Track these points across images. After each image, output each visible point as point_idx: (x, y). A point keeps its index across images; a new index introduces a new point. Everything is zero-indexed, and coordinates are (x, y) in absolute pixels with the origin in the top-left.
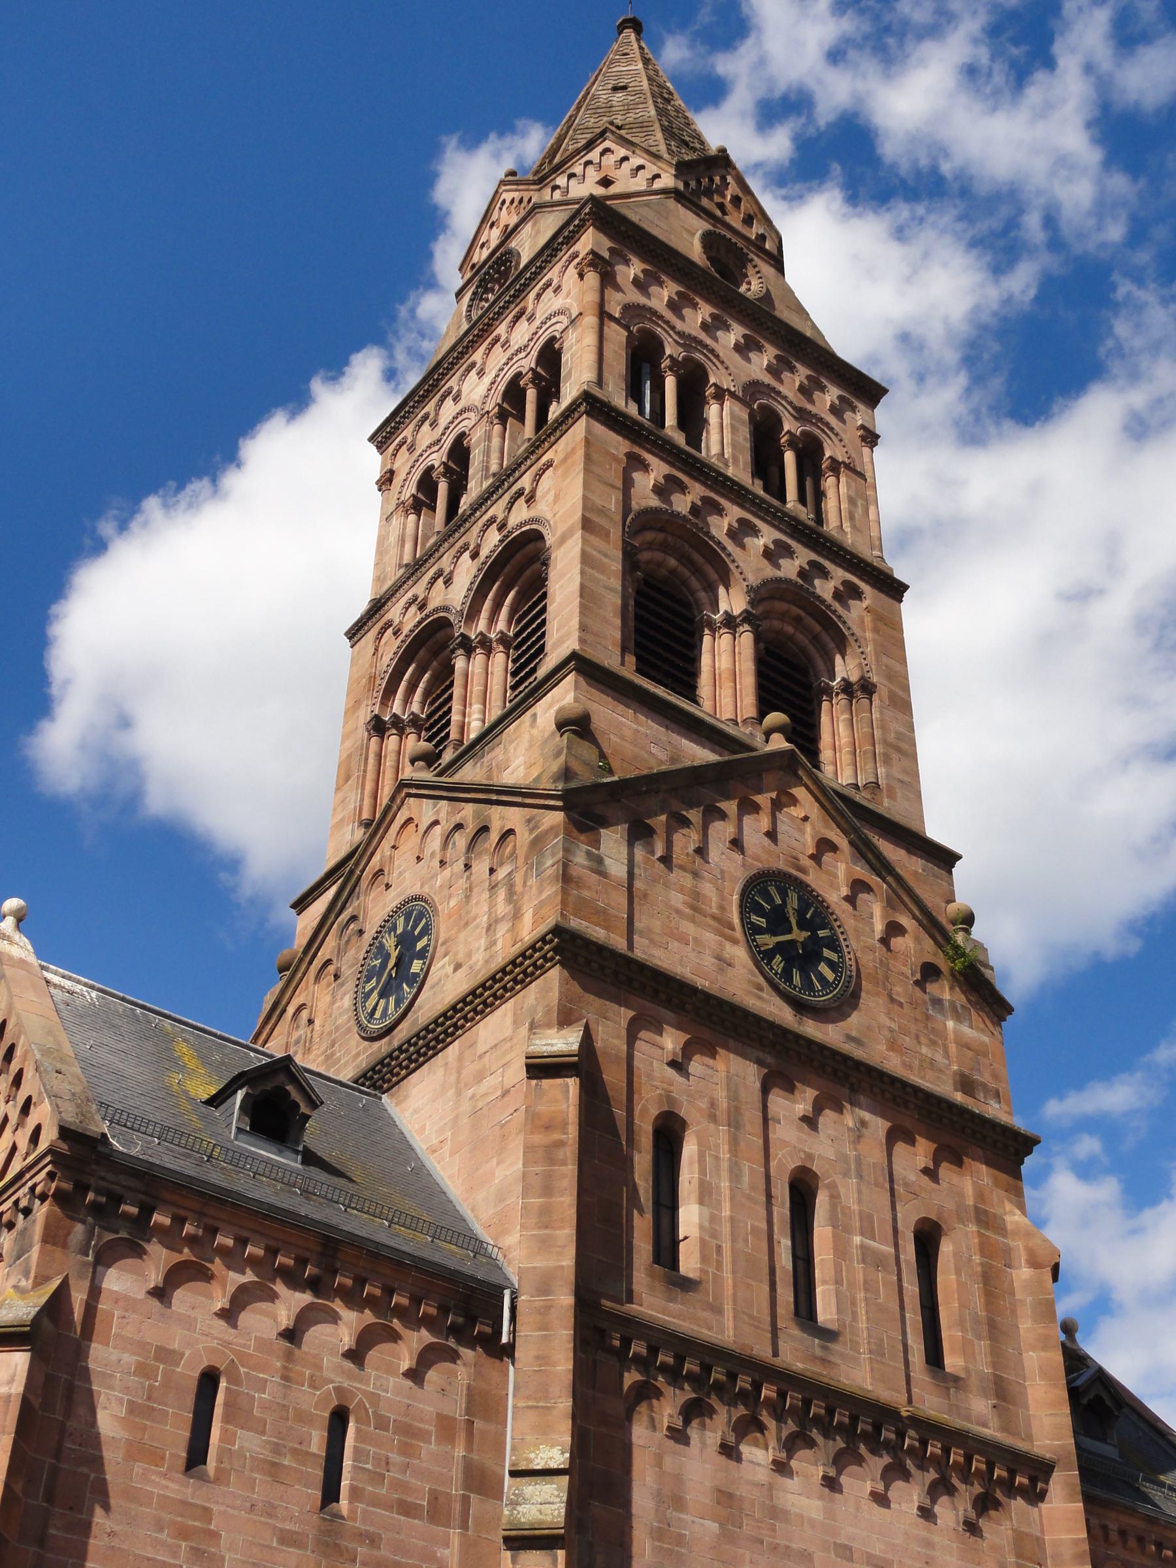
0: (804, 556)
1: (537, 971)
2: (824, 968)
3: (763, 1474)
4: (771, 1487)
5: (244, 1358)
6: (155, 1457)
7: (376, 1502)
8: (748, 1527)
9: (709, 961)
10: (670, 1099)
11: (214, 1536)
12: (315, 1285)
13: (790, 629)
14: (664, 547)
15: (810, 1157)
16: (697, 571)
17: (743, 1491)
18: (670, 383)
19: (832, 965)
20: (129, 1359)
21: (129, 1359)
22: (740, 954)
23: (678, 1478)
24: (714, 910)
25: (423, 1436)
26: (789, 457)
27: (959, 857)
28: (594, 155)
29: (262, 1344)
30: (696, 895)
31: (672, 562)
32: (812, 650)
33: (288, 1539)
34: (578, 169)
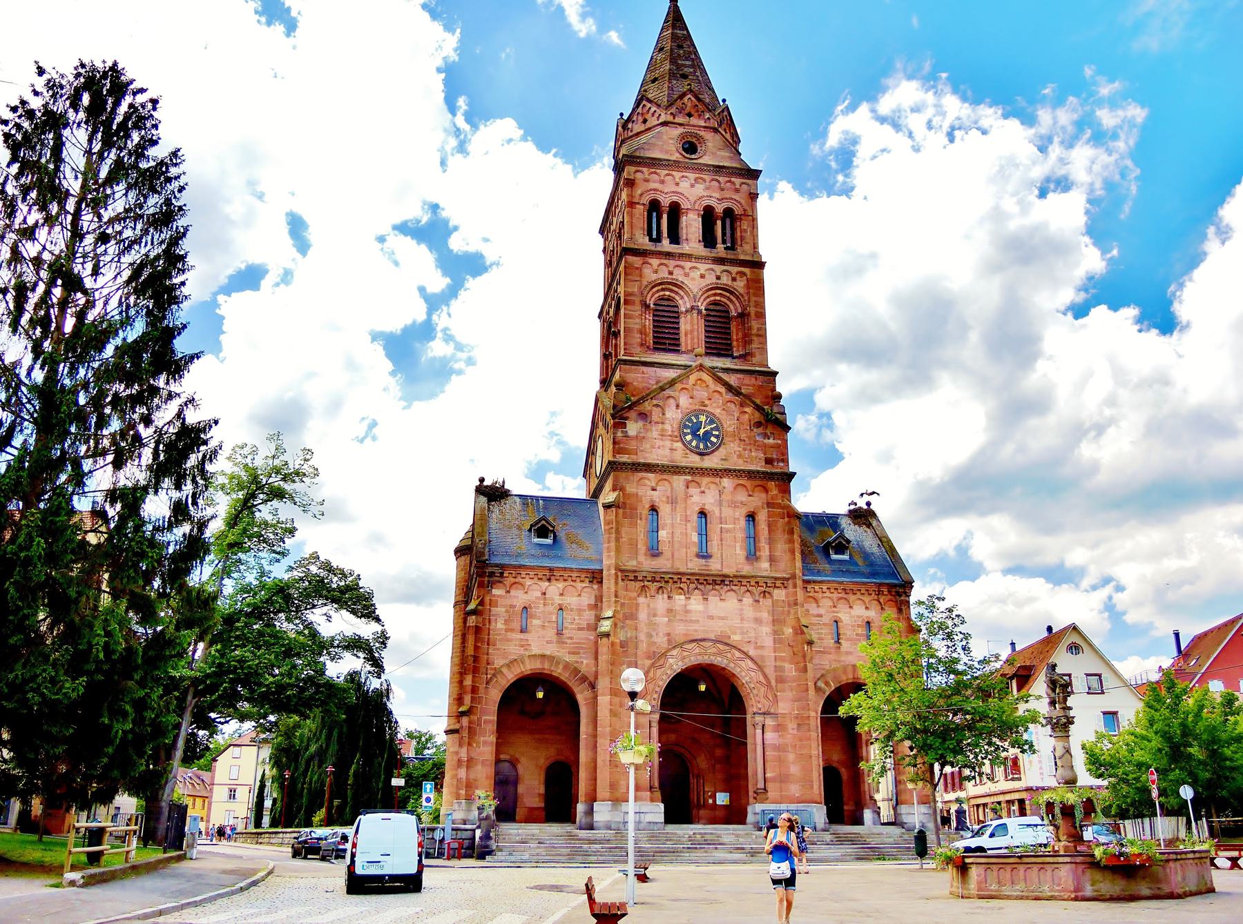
0: (719, 268)
1: (609, 474)
2: (713, 439)
3: (683, 602)
4: (686, 605)
5: (534, 602)
6: (512, 630)
7: (572, 629)
8: (678, 617)
9: (667, 452)
10: (652, 501)
11: (530, 645)
12: (549, 580)
13: (718, 298)
14: (663, 290)
15: (704, 504)
16: (677, 293)
17: (677, 608)
18: (665, 216)
19: (717, 437)
20: (504, 610)
21: (504, 610)
22: (679, 445)
23: (655, 609)
24: (670, 433)
25: (585, 610)
26: (719, 223)
27: (777, 373)
28: (639, 110)
29: (537, 598)
30: (663, 430)
31: (667, 293)
32: (728, 302)
33: (548, 642)
34: (635, 118)
